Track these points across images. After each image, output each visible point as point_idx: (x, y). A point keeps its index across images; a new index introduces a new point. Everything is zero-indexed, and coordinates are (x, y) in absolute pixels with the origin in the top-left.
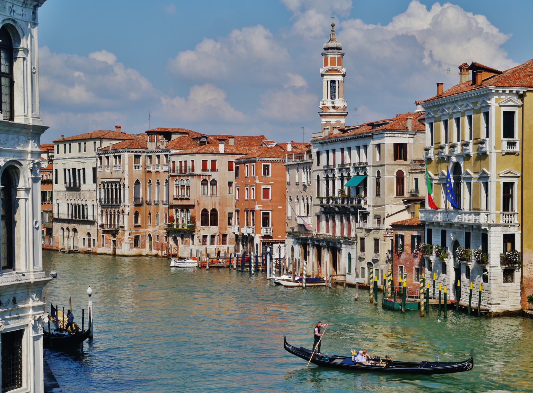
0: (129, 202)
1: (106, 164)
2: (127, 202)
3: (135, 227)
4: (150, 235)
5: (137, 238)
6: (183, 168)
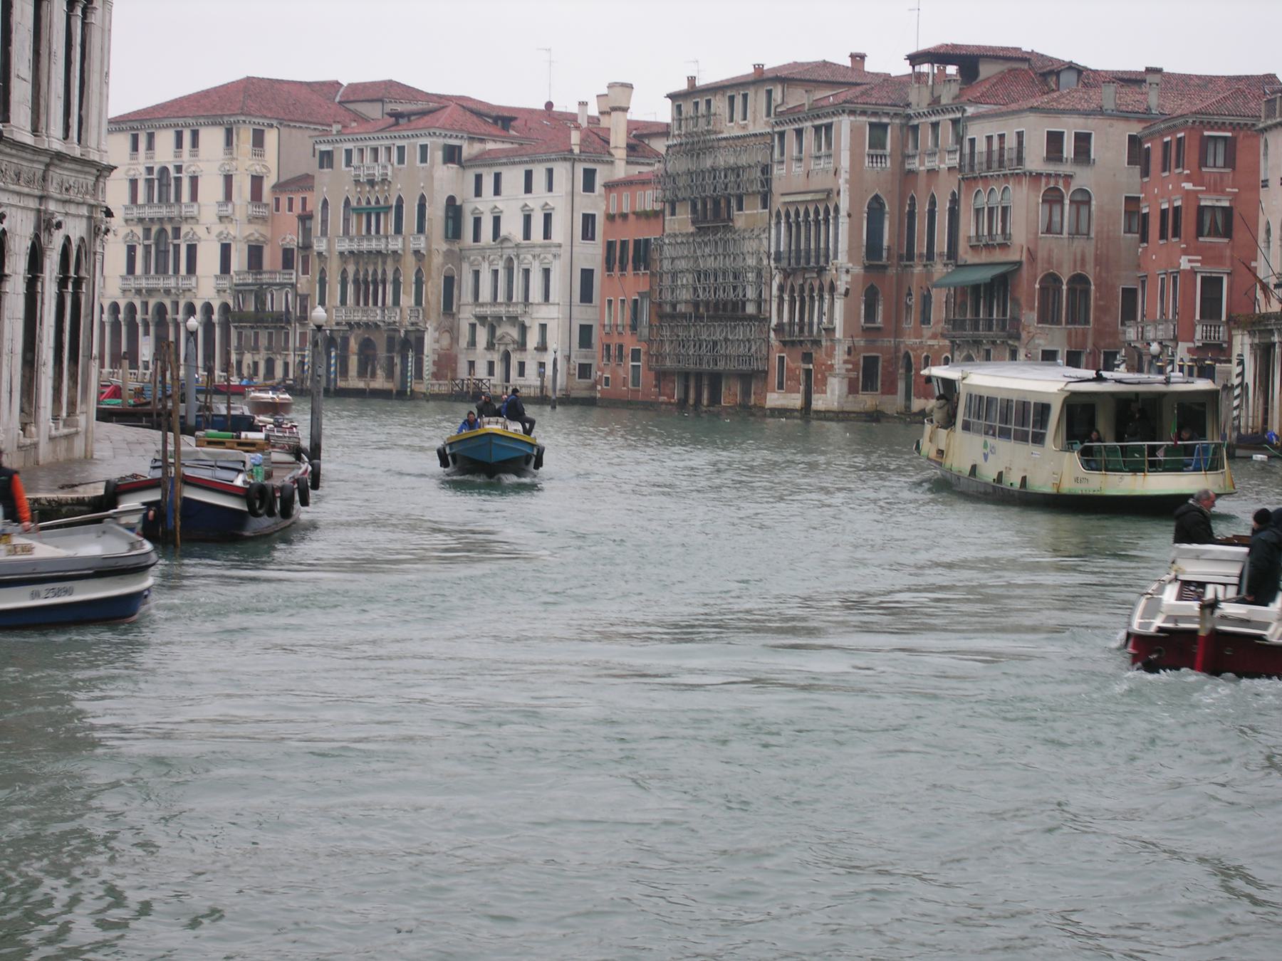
0: (851, 259)
1: (795, 153)
2: (843, 259)
3: (866, 330)
4: (907, 356)
5: (870, 363)
6: (995, 157)
